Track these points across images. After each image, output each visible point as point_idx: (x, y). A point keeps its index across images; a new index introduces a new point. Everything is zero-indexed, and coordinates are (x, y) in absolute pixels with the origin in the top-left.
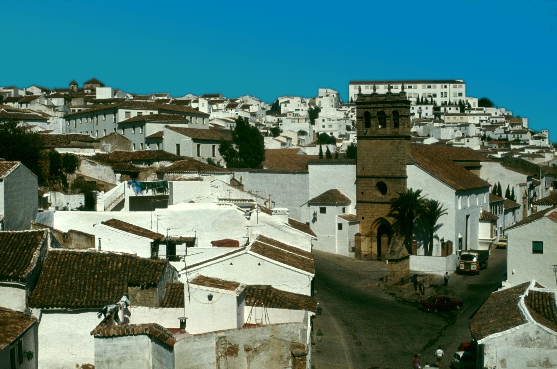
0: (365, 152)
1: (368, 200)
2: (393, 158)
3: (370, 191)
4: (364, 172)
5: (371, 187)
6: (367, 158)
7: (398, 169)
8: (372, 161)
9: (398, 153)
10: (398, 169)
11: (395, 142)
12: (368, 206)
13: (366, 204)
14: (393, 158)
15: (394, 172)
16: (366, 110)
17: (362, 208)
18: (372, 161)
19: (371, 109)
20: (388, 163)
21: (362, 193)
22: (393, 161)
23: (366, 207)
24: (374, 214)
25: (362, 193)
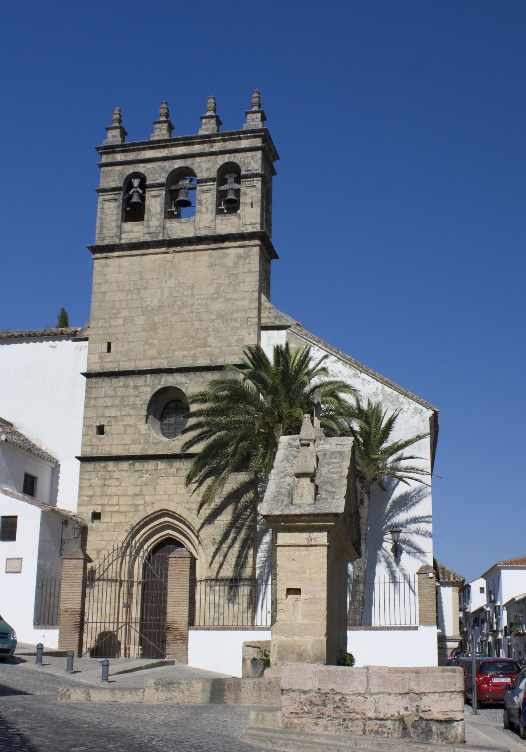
0: (122, 296)
1: (116, 451)
2: (216, 306)
3: (129, 421)
4: (109, 358)
5: (134, 407)
6: (125, 313)
7: (233, 339)
8: (141, 320)
9: (234, 291)
10: (233, 339)
11: (226, 256)
12: (117, 475)
13: (111, 465)
14: (216, 306)
15: (217, 351)
16: (130, 169)
17: (96, 482)
18: (141, 320)
19: (149, 166)
20: (197, 325)
21: (101, 430)
22: (214, 317)
23: (111, 478)
24: (139, 501)
25: (101, 430)
